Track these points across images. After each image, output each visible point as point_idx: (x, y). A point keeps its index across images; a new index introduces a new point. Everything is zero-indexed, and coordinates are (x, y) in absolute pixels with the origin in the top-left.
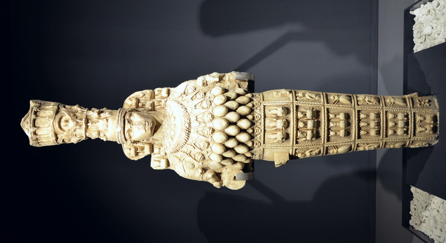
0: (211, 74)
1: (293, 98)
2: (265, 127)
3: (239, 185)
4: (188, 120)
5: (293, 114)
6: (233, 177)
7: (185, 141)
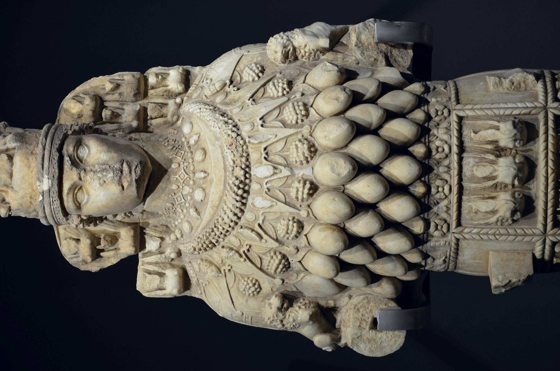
0: (307, 28)
1: (546, 93)
2: (460, 179)
3: (390, 342)
4: (244, 160)
5: (546, 140)
6: (370, 320)
7: (235, 218)
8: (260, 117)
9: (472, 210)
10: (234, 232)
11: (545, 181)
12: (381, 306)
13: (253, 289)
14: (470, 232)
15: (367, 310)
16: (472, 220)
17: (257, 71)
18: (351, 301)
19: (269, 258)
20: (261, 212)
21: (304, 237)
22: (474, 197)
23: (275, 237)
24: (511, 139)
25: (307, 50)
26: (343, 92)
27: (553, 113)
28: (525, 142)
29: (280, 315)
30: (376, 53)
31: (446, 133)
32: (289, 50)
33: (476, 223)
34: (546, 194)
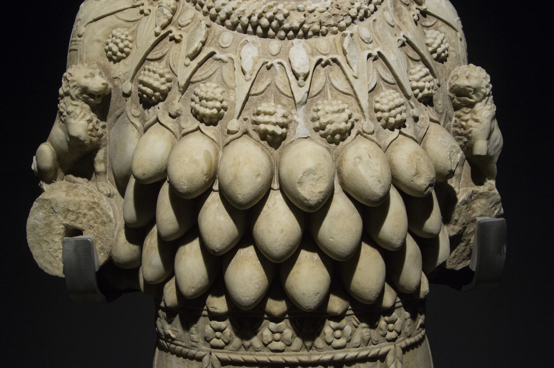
0: (495, 122)
3: (50, 254)
4: (316, 27)
7: (222, 15)
8: (383, 53)
10: (200, 15)
12: (99, 242)
13: (115, 49)
15: (92, 222)
17: (439, 50)
18: (105, 198)
19: (161, 71)
20: (233, 56)
21: (195, 126)
23: (193, 79)
25: (471, 123)
26: (427, 184)
29: (77, 92)
30: (464, 221)
31: (363, 339)
32: (471, 98)
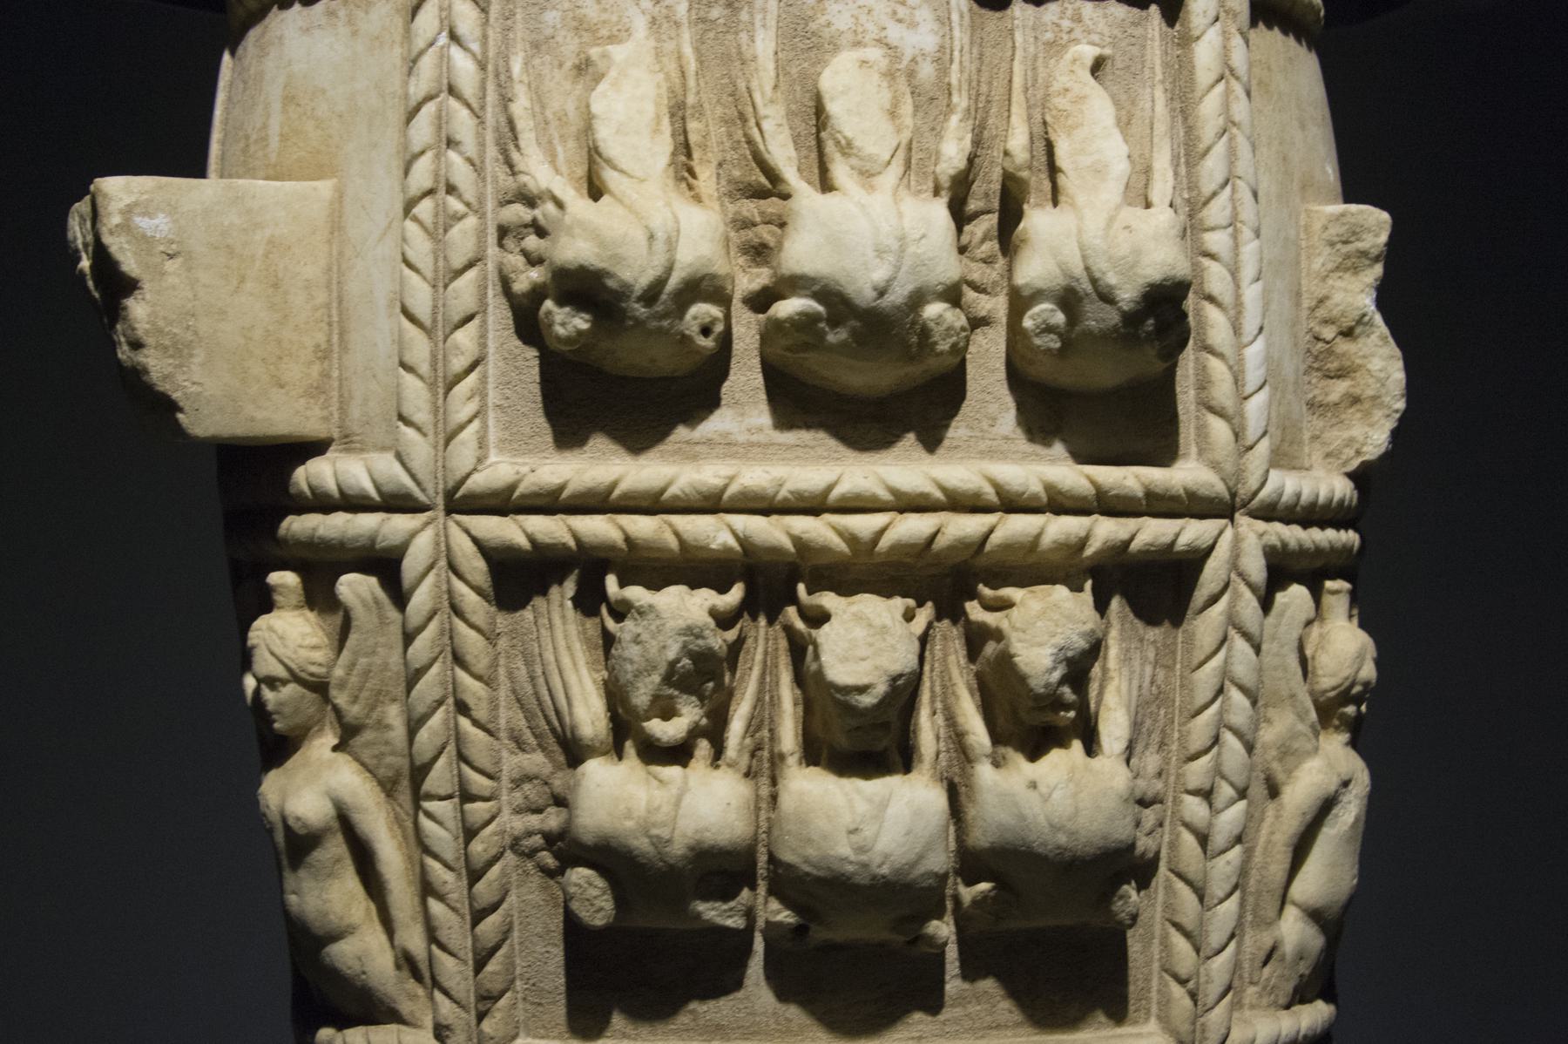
5: (1058, 503)
9: (598, 41)
11: (799, 495)
14: (454, 37)
16: (536, 46)
22: (688, 51)
24: (1078, 270)
27: (1212, 548)
28: (1043, 371)
33: (517, 67)
34: (711, 504)
